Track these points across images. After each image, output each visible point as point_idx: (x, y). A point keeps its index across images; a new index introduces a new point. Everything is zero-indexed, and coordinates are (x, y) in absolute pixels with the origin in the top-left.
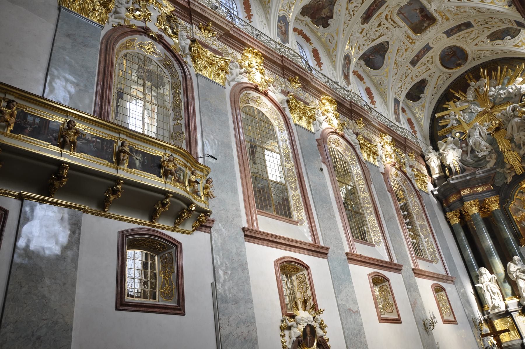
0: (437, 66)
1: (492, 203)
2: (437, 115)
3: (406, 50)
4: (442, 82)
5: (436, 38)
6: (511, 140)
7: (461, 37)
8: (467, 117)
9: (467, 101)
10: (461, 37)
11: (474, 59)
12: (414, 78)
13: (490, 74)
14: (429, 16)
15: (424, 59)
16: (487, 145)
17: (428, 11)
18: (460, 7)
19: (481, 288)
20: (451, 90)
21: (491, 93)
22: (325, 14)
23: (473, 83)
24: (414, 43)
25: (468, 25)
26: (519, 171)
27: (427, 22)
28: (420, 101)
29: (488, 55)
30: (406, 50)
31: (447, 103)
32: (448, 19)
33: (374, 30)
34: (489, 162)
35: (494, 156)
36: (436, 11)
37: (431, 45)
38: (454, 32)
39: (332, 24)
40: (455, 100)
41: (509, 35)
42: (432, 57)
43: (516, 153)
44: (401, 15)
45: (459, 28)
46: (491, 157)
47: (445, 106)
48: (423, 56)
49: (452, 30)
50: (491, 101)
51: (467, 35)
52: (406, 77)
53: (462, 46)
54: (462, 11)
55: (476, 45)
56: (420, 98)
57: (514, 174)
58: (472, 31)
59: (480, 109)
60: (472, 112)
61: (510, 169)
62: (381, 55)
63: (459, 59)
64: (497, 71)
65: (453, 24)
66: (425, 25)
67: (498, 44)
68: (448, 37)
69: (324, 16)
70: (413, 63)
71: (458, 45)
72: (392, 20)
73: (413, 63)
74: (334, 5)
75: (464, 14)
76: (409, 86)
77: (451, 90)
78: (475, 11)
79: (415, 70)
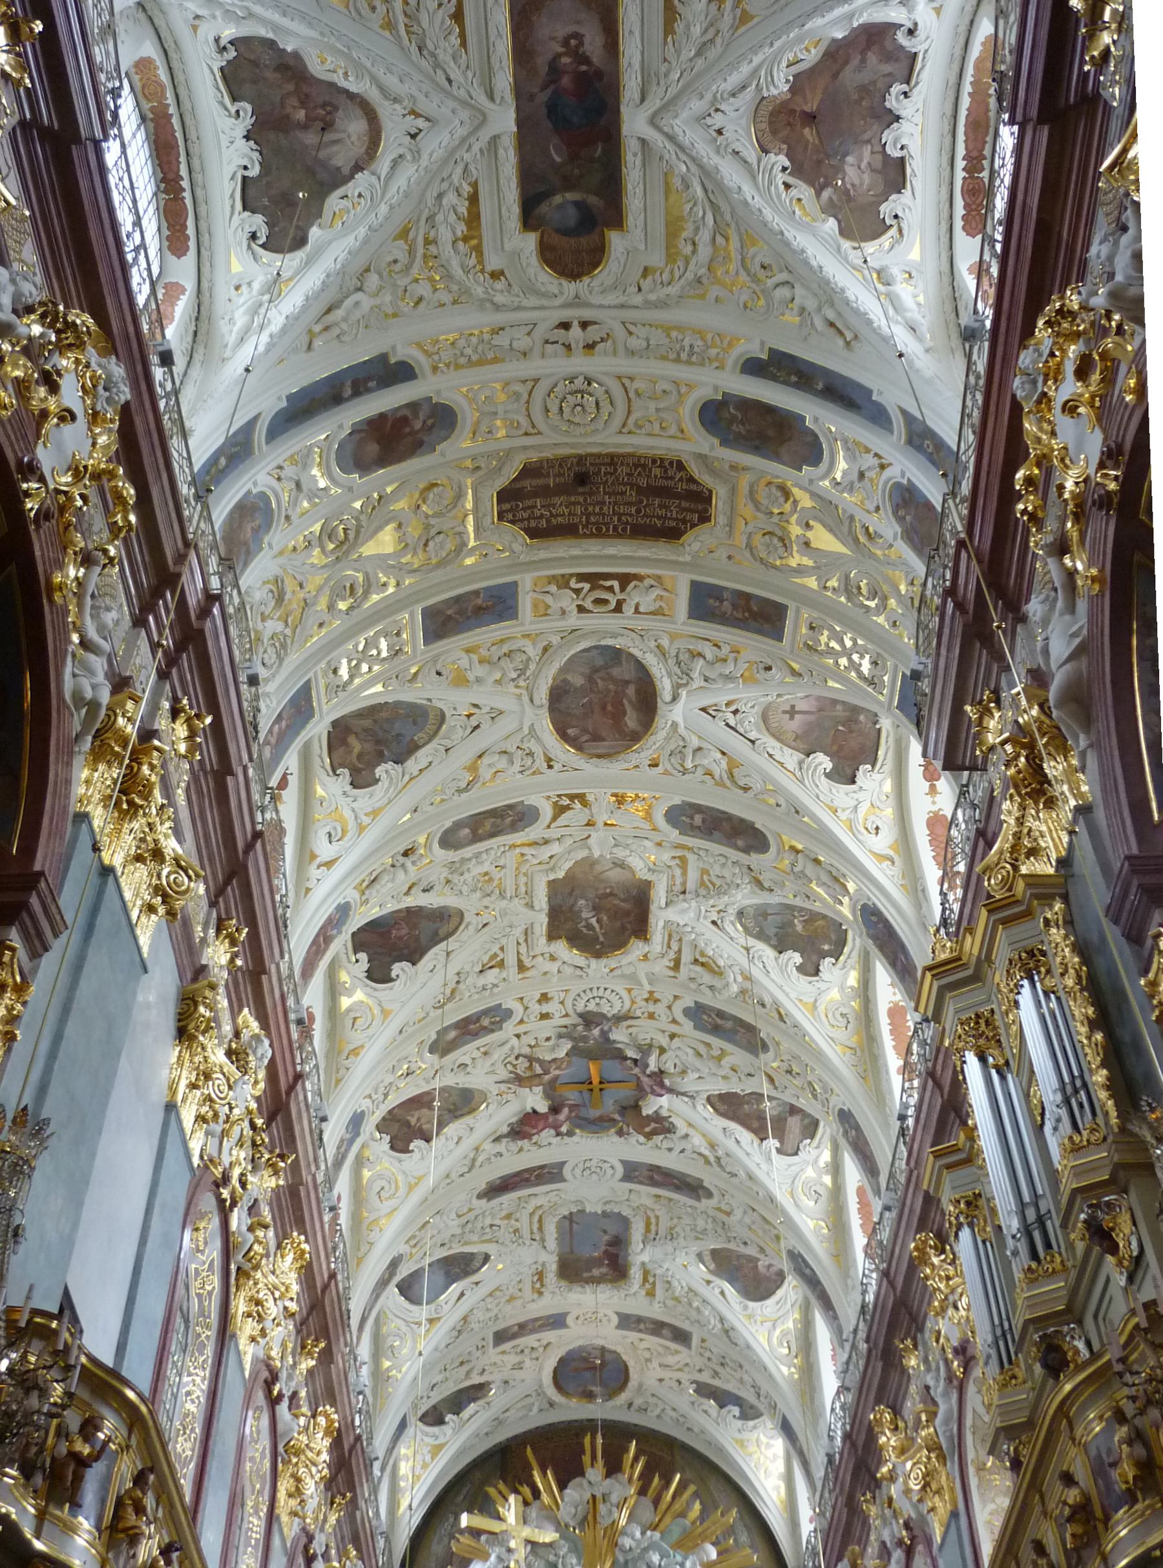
0: (541, 1369)
3: (512, 1299)
4: (520, 1414)
5: (593, 1315)
7: (644, 1345)
10: (644, 1345)
11: (630, 1405)
12: (475, 1371)
14: (620, 1261)
15: (529, 1340)
17: (627, 1255)
18: (696, 1294)
20: (529, 1449)
22: (419, 1119)
23: (595, 1473)
24: (540, 1293)
25: (681, 1337)
27: (604, 1270)
28: (435, 1430)
29: (667, 1419)
30: (512, 1299)
32: (651, 1294)
33: (488, 1221)
36: (643, 1264)
37: (570, 1320)
38: (642, 1326)
39: (416, 1155)
41: (740, 1406)
42: (548, 1344)
44: (567, 1223)
45: (657, 1328)
47: (491, 1491)
48: (533, 1331)
49: (639, 1320)
51: (660, 1349)
52: (462, 1363)
53: (631, 1364)
54: (695, 1304)
55: (661, 1380)
56: (440, 1421)
58: (677, 1352)
62: (447, 1274)
63: (603, 1384)
65: (655, 1311)
66: (596, 1272)
67: (706, 1412)
68: (618, 1327)
69: (413, 1121)
70: (501, 1337)
71: (625, 1358)
72: (540, 1221)
73: (501, 1337)
74: (457, 1117)
75: (694, 1314)
76: (450, 1388)
77: (529, 1449)
78: (719, 1326)
79: (493, 1354)
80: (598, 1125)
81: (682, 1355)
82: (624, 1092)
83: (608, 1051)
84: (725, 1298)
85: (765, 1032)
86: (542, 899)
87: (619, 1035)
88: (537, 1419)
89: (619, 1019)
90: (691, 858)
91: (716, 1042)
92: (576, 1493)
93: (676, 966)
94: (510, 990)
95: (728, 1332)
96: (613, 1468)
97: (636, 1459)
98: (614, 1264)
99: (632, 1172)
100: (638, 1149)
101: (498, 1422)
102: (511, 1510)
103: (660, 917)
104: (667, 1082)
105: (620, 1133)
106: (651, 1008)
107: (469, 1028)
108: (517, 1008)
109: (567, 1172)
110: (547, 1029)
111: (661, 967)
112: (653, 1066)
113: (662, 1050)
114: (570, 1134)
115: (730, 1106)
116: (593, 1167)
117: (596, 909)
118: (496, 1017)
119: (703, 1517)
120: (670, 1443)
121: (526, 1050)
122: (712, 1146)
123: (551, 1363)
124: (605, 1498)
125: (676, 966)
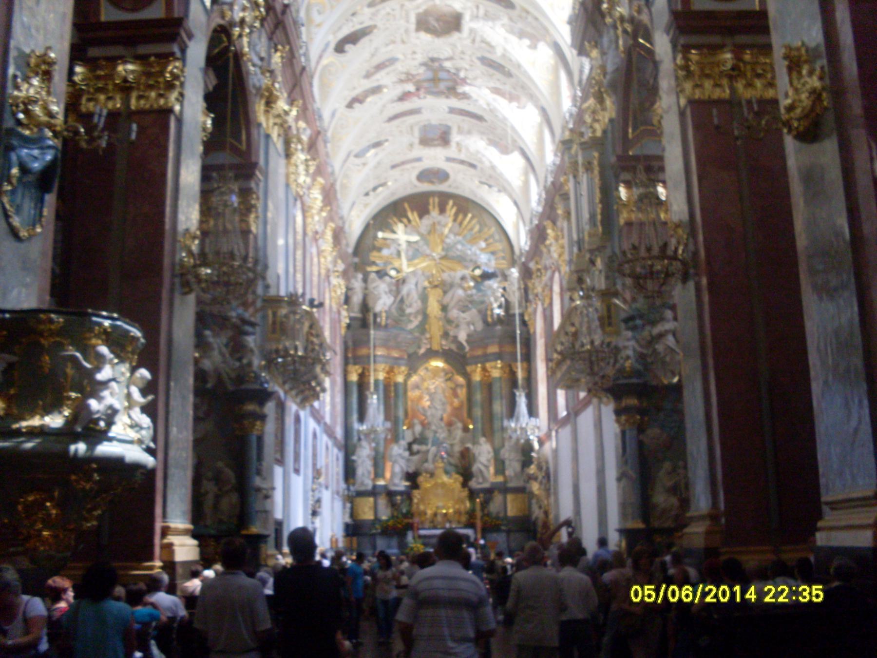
1: (399, 373)
2: (380, 235)
6: (444, 308)
8: (410, 253)
9: (419, 234)
13: (456, 215)
16: (419, 303)
19: (354, 461)
20: (406, 205)
21: (448, 241)
25: (473, 166)
26: (436, 347)
31: (395, 219)
32: (460, 151)
34: (410, 321)
35: (420, 318)
40: (405, 220)
43: (441, 323)
45: (462, 162)
46: (416, 317)
50: (443, 249)
57: (428, 346)
59: (428, 252)
60: (417, 250)
61: (427, 339)
64: (465, 216)
65: (462, 157)
66: (436, 142)
70: (394, 167)
73: (394, 167)
77: (406, 205)
80: (438, 94)
81: (472, 171)
82: (450, 84)
83: (442, 68)
84: (491, 155)
85: (514, 71)
86: (413, 19)
87: (447, 65)
88: (410, 191)
89: (447, 59)
90: (481, 7)
91: (491, 71)
92: (426, 221)
93: (474, 41)
94: (397, 51)
95: (493, 168)
96: (442, 210)
97: (452, 207)
98: (444, 139)
99: (452, 111)
100: (454, 103)
101: (393, 194)
102: (400, 228)
103: (467, 24)
104: (468, 81)
105: (447, 97)
106: (462, 56)
107: (380, 67)
108: (400, 56)
109: (423, 111)
110: (416, 63)
111: (468, 42)
112: (462, 74)
113: (466, 70)
114: (425, 97)
115: (496, 91)
116: (435, 109)
117: (438, 20)
118: (392, 61)
119: (480, 231)
120: (467, 200)
121: (405, 70)
122: (488, 105)
123: (415, 173)
124: (439, 223)
125: (474, 41)
